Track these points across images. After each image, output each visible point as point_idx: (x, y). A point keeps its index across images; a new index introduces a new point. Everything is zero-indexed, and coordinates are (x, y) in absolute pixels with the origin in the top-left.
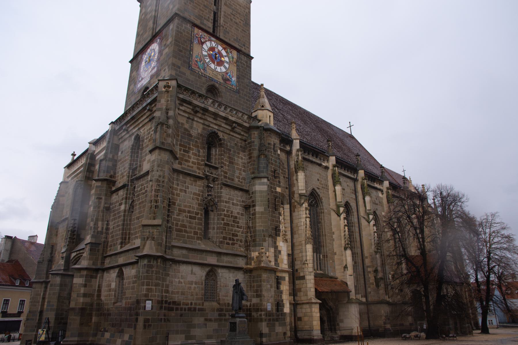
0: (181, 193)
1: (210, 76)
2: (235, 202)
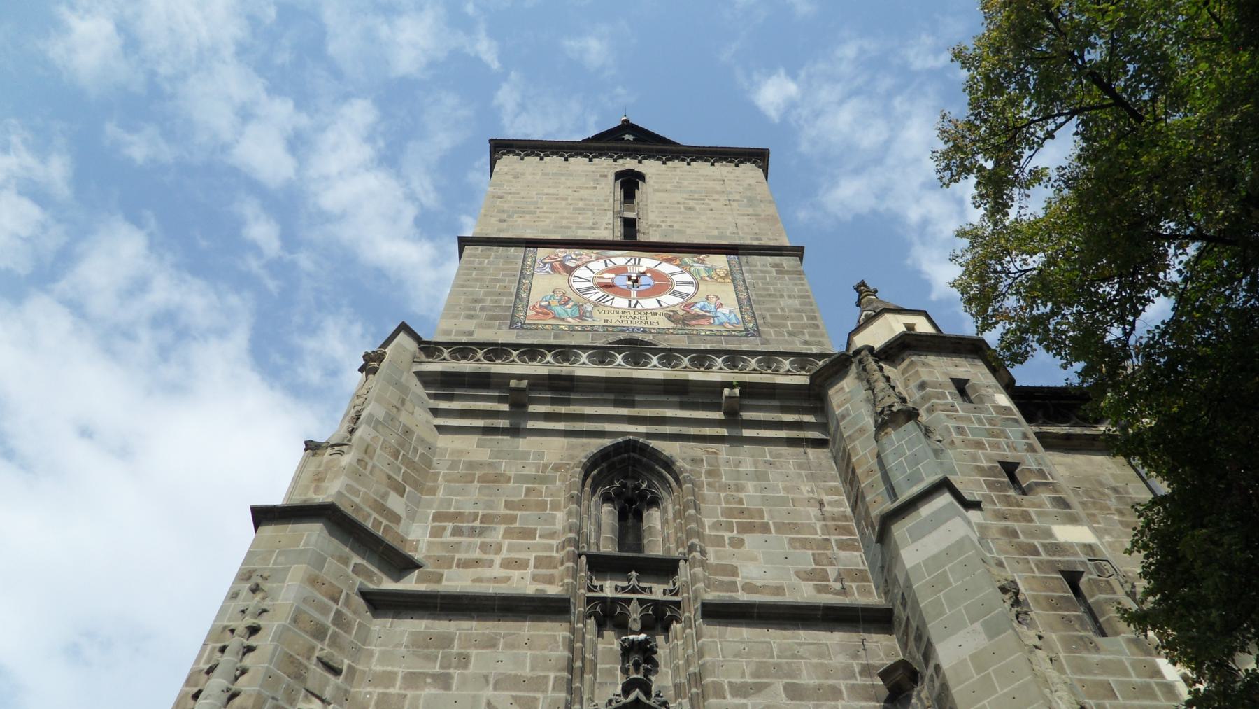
0: (410, 693)
1: (609, 324)
2: (807, 679)
